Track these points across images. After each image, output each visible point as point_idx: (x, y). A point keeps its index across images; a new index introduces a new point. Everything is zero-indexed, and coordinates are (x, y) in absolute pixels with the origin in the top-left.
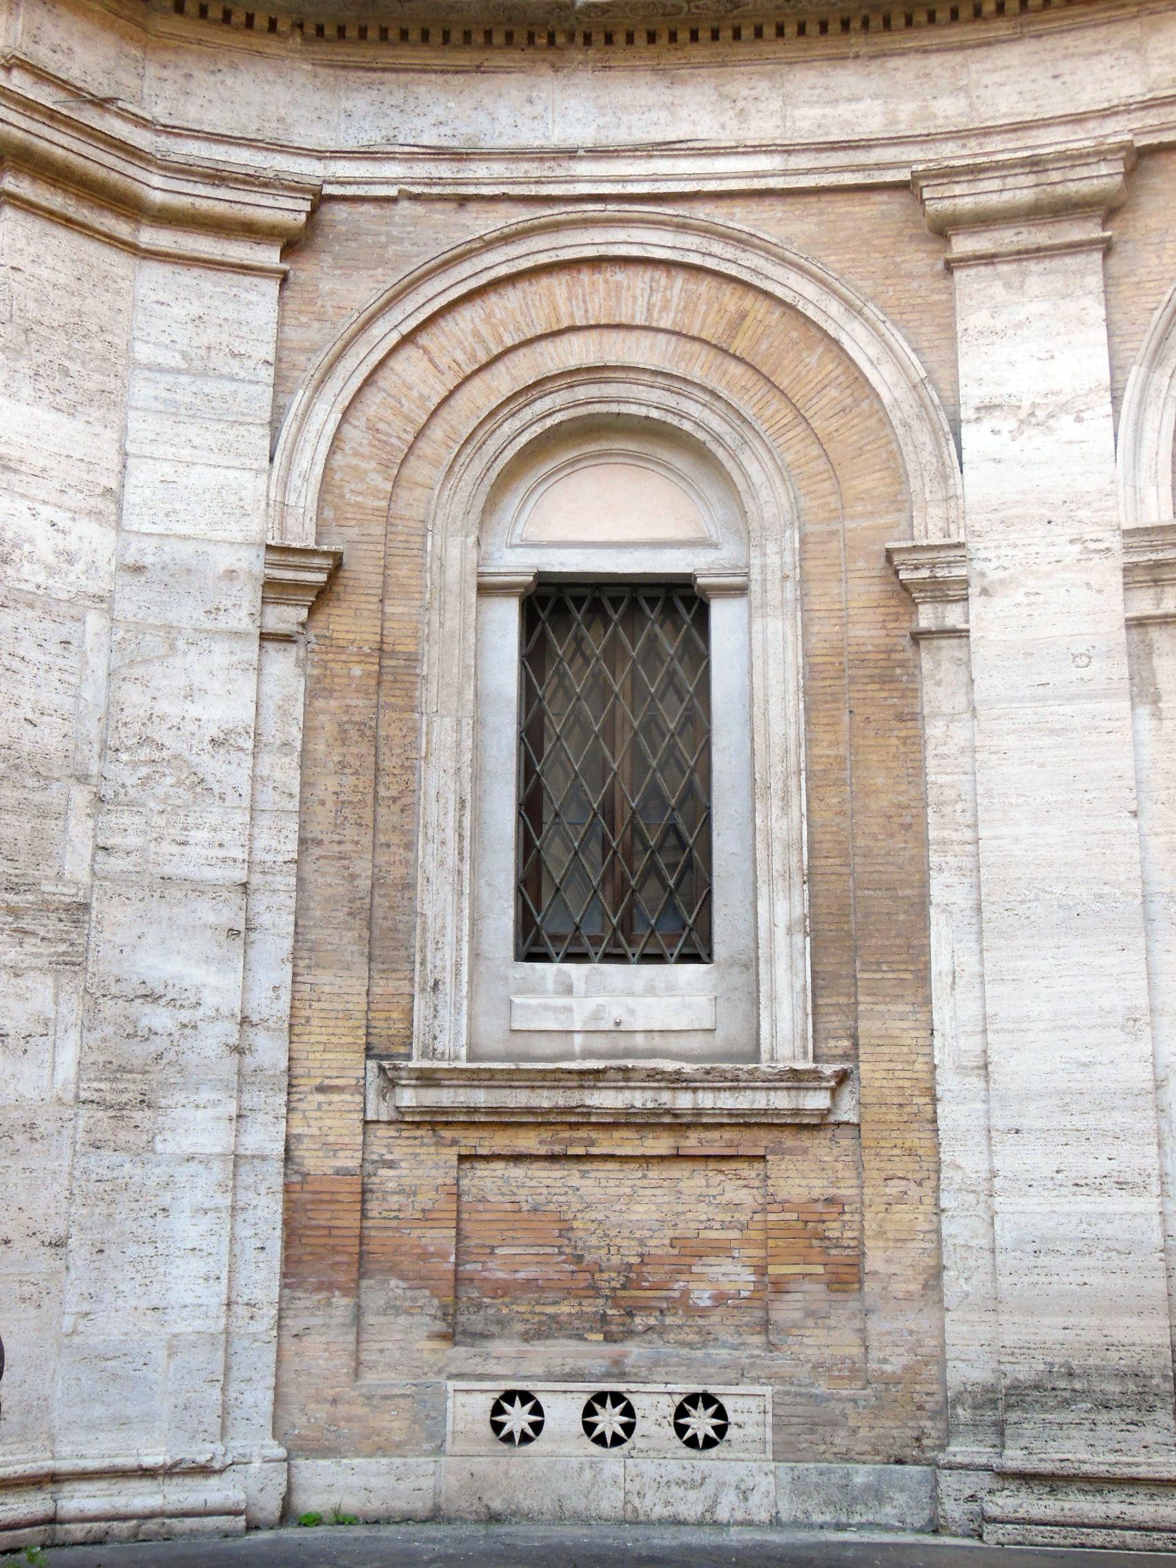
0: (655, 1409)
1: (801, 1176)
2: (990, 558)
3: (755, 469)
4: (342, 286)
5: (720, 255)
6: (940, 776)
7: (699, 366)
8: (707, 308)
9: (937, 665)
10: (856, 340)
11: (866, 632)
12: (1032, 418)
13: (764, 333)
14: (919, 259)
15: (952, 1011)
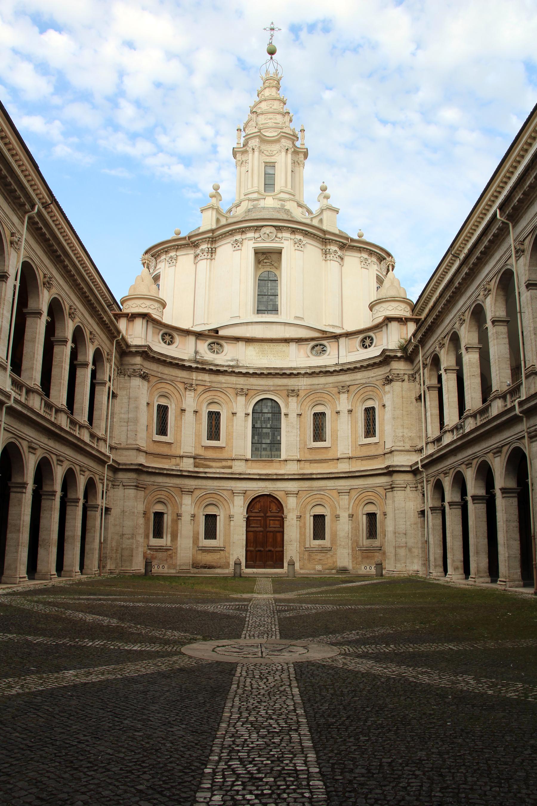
0: (161, 566)
1: (170, 552)
2: (183, 515)
3: (169, 506)
4: (147, 492)
5: (168, 491)
6: (179, 528)
7: (166, 498)
8: (167, 494)
9: (179, 521)
10: (176, 498)
11: (175, 518)
12: (186, 505)
13: (170, 496)
14: (180, 493)
15: (179, 543)
